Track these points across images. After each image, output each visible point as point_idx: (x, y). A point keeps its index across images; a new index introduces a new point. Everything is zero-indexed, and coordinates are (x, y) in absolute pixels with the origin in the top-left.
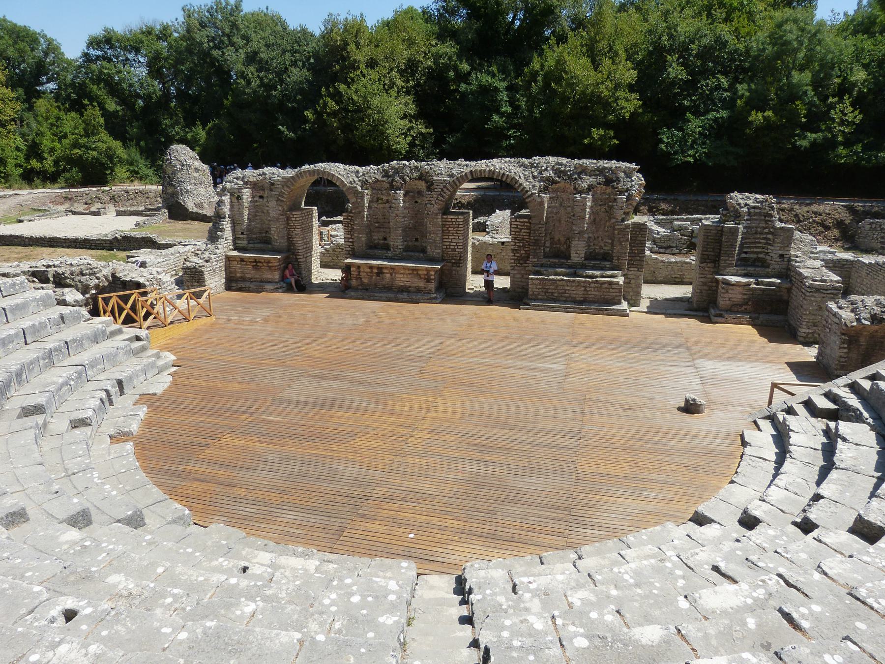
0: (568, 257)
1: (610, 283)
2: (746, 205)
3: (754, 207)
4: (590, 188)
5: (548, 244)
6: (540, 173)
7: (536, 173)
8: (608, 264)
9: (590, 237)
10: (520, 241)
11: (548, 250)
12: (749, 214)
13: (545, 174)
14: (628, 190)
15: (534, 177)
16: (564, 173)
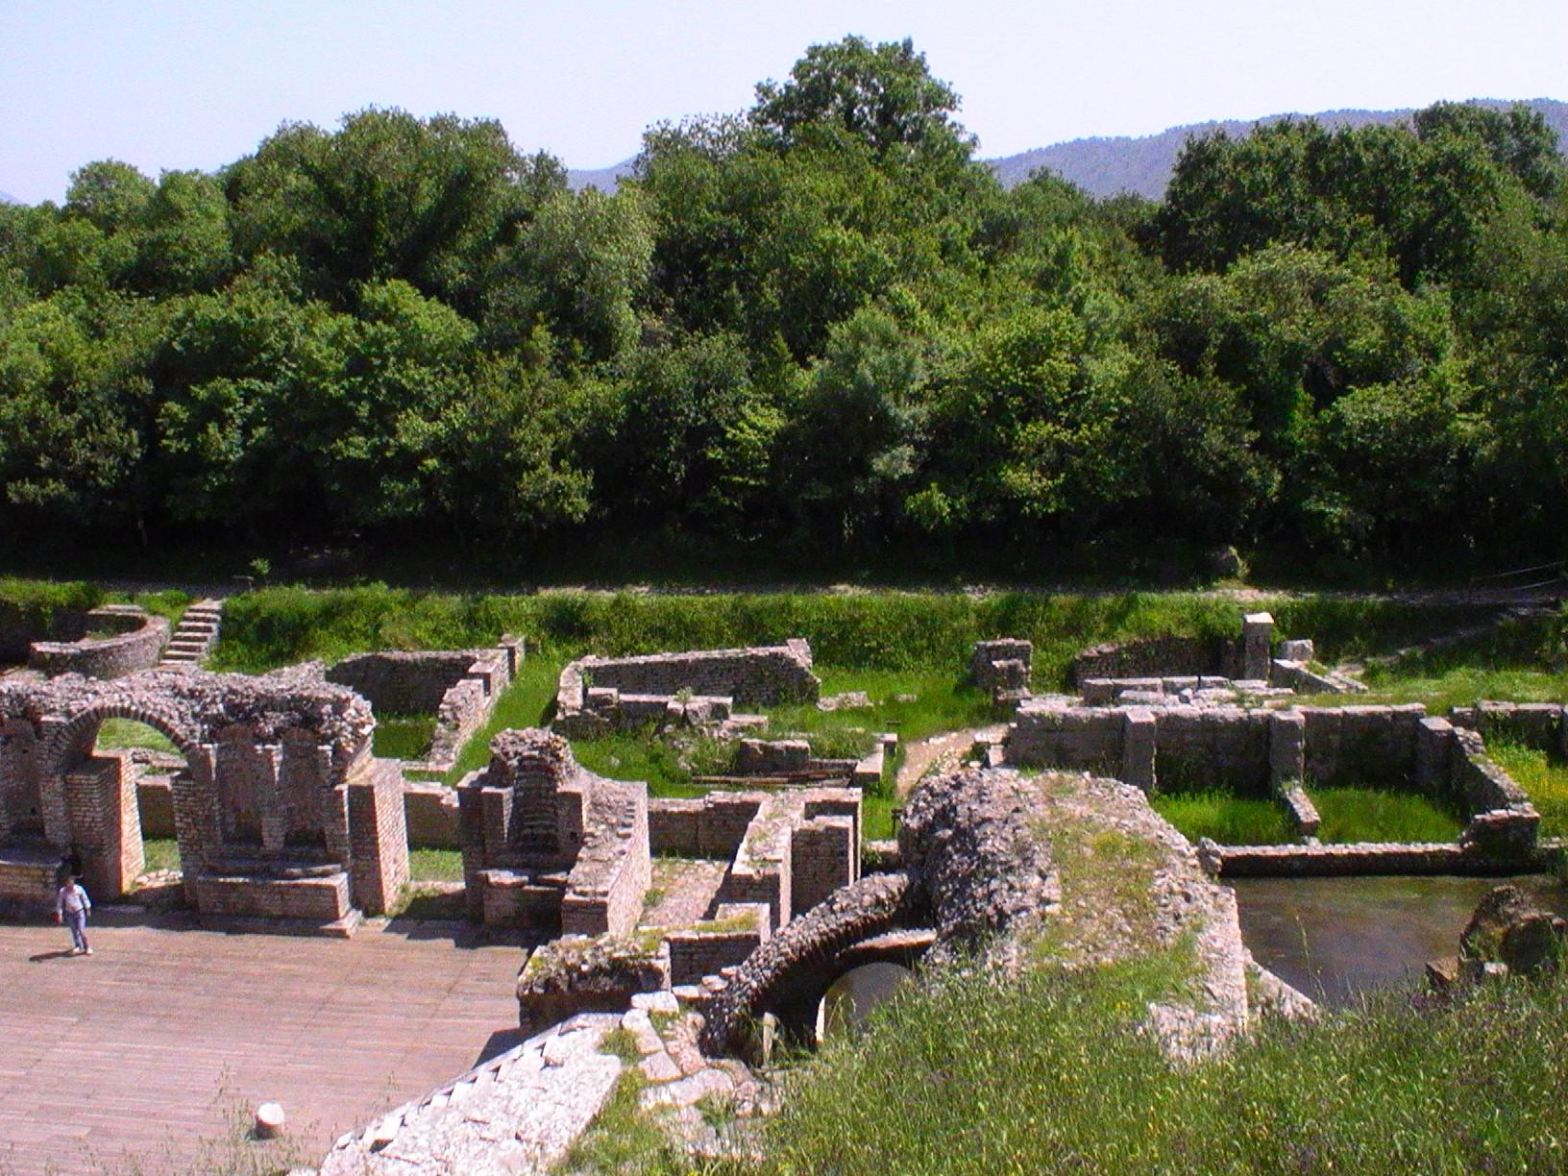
0: (260, 842)
1: (318, 887)
2: (516, 754)
3: (531, 758)
4: (279, 733)
5: (230, 819)
6: (204, 708)
7: (197, 709)
8: (318, 852)
9: (290, 810)
10: (187, 815)
11: (232, 829)
12: (521, 767)
13: (213, 710)
14: (334, 735)
15: (195, 716)
16: (240, 707)
